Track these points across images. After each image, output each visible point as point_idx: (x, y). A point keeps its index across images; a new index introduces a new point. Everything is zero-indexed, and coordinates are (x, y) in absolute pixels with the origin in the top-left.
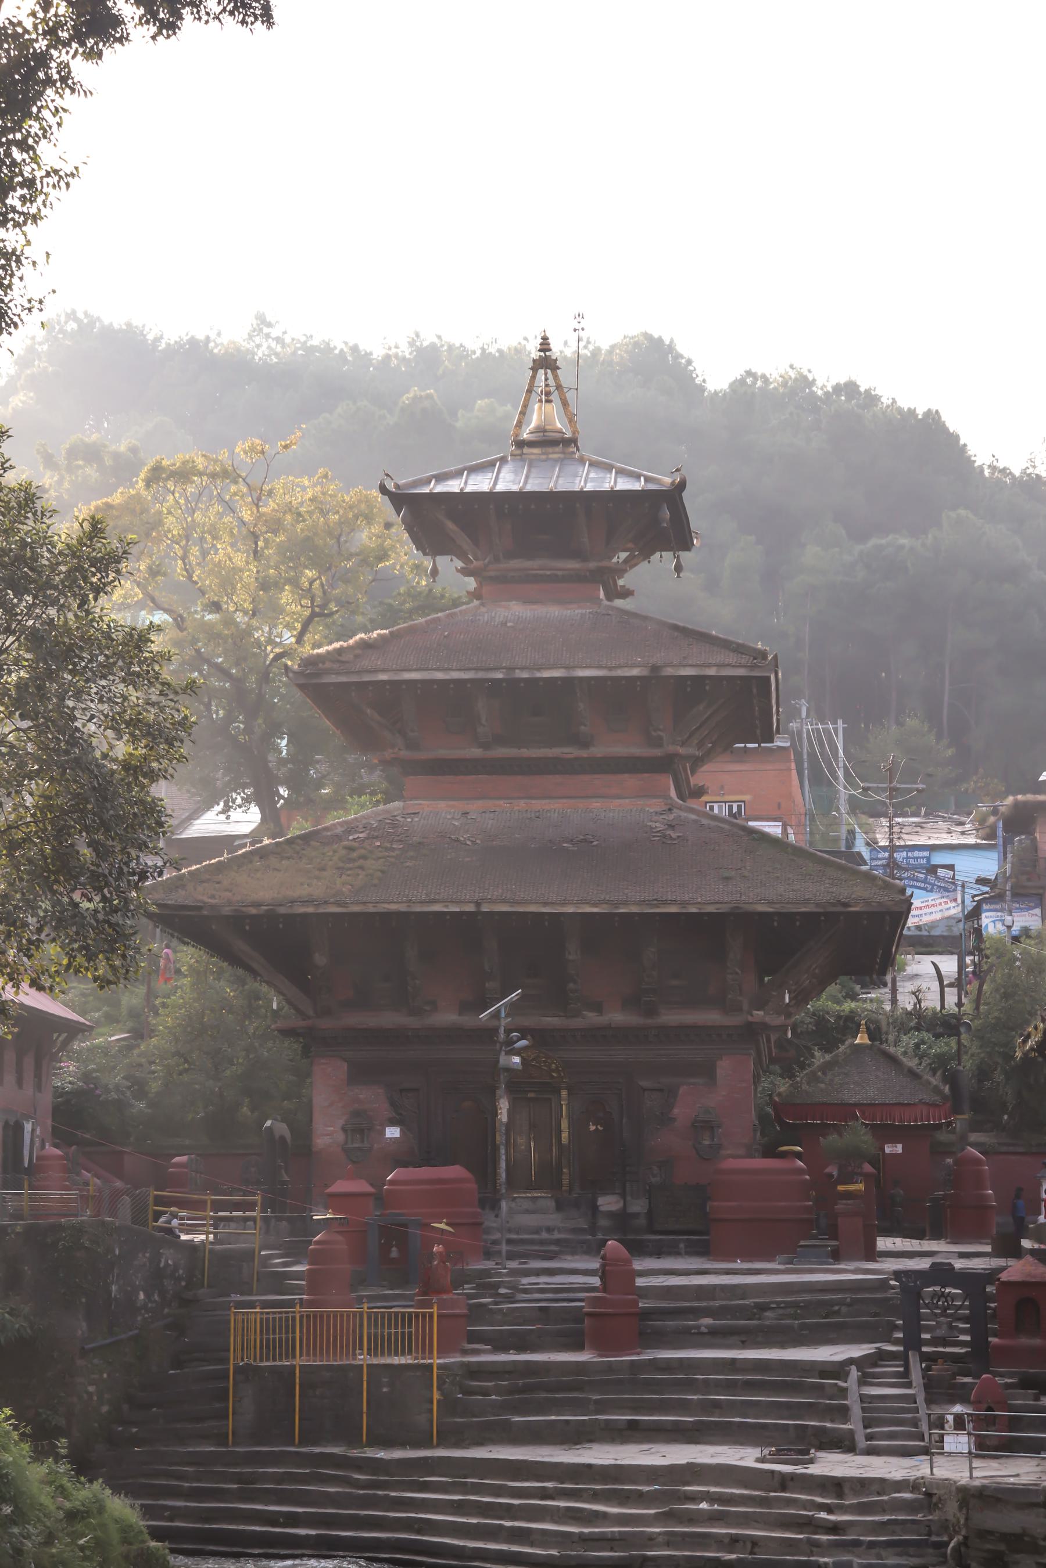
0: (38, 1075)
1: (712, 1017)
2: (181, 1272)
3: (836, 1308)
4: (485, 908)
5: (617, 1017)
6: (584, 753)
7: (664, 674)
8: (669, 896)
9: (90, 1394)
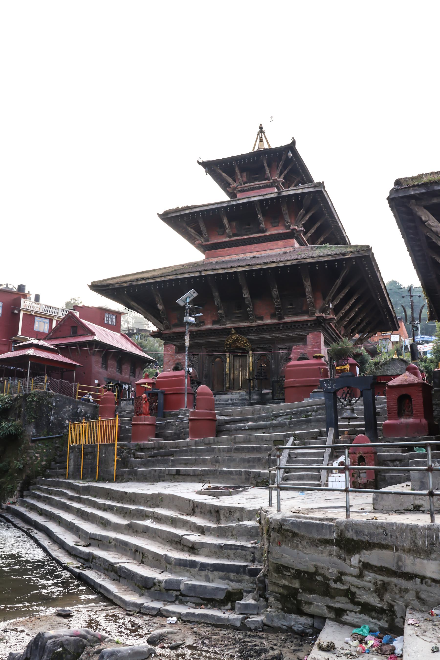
2: (88, 415)
3: (310, 413)
4: (203, 274)
5: (269, 321)
6: (263, 235)
7: (282, 195)
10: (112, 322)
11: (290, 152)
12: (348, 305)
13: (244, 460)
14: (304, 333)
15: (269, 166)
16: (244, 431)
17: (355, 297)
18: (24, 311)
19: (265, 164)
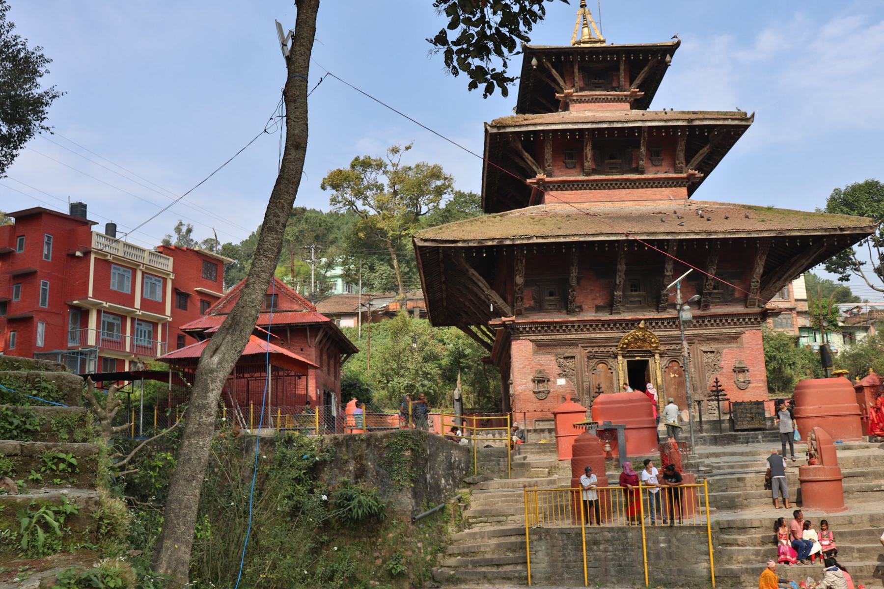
0: (335, 372)
1: (739, 309)
4: (630, 238)
6: (643, 176)
8: (741, 228)
9: (419, 549)
14: (738, 330)
18: (95, 253)
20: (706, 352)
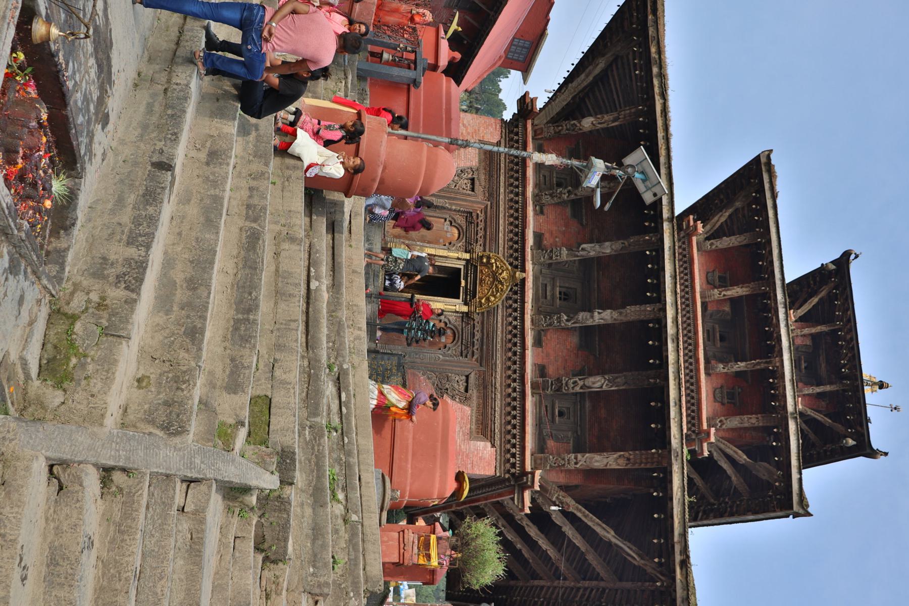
3: (341, 496)
10: (515, 52)
11: (854, 443)
12: (536, 534)
13: (202, 262)
15: (819, 396)
16: (305, 273)
17: (552, 552)
19: (828, 388)
20: (467, 382)
